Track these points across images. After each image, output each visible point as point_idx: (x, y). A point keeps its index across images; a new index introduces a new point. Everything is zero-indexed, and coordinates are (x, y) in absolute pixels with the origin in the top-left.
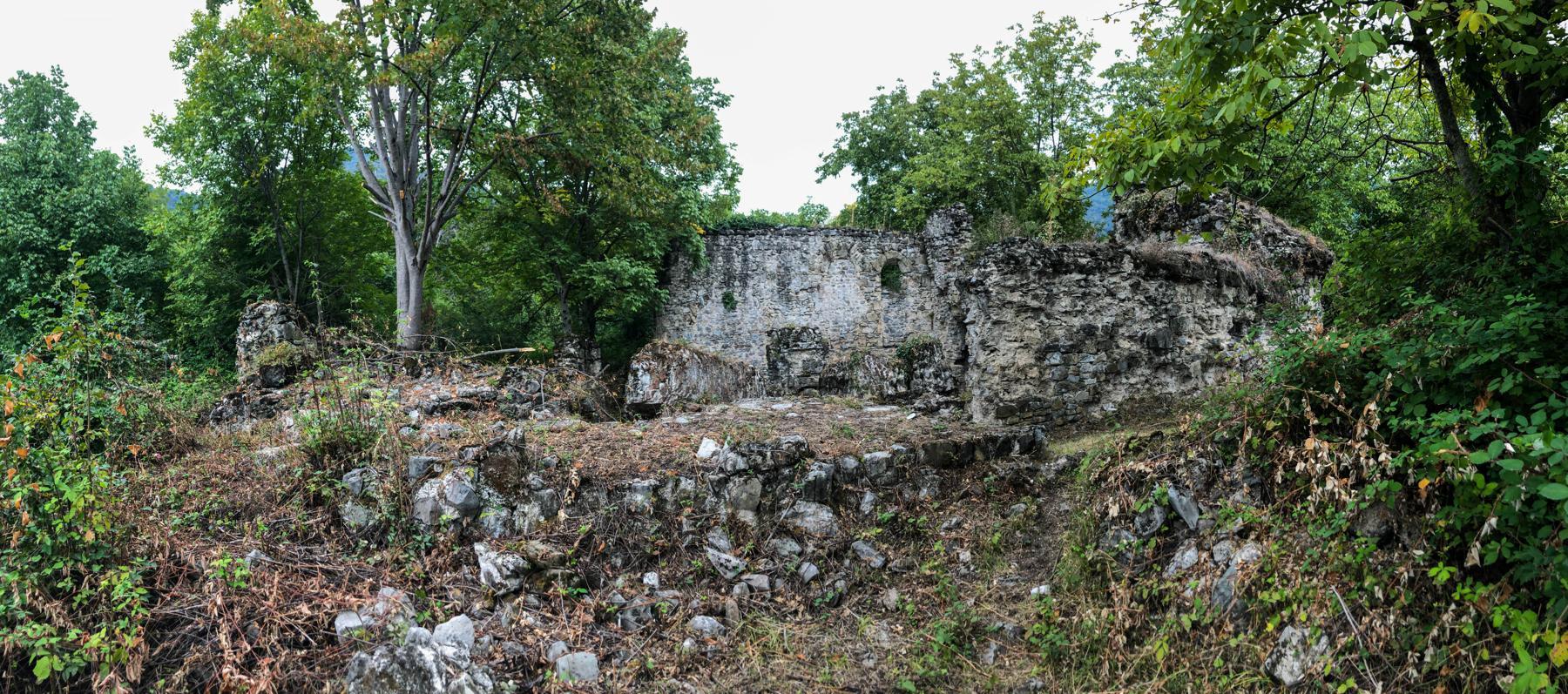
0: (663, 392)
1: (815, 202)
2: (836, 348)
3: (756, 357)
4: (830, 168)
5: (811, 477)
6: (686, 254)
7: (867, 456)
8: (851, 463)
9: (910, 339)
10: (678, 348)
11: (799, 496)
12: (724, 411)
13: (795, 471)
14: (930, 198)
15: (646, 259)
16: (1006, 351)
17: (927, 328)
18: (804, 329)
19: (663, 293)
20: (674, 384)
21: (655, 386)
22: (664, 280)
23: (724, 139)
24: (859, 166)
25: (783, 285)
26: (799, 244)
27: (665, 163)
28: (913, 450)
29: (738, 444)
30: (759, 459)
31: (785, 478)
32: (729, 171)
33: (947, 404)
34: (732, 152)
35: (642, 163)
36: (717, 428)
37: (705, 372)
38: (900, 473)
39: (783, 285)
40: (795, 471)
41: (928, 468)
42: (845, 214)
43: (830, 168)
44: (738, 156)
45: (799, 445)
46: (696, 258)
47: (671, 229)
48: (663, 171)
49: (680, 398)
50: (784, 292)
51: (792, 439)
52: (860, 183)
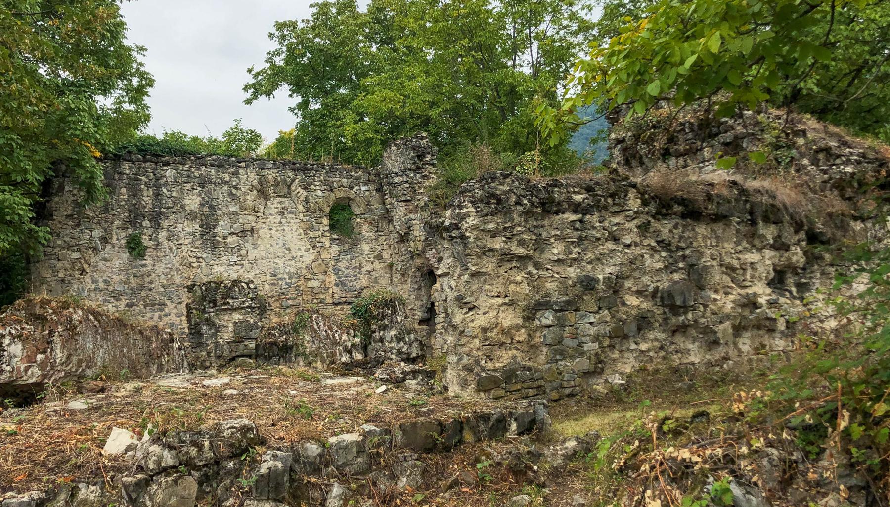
0: (42, 366)
1: (246, 126)
2: (275, 306)
3: (174, 318)
4: (262, 86)
5: (263, 470)
6: (76, 181)
7: (333, 440)
8: (313, 449)
9: (365, 294)
10: (65, 306)
11: (248, 494)
12: (138, 390)
13: (241, 463)
14: (385, 126)
15: (15, 184)
16: (485, 309)
17: (384, 281)
18: (236, 283)
19: (42, 232)
20: (59, 355)
21: (30, 359)
22: (42, 213)
23: (129, 40)
24: (298, 87)
25: (208, 226)
26: (227, 177)
27: (44, 59)
28: (388, 432)
29: (164, 433)
30: (194, 451)
31: (229, 473)
32: (135, 81)
33: (415, 374)
34: (140, 58)
35: (11, 56)
36: (135, 415)
37: (105, 338)
38: (374, 458)
39: (208, 226)
40: (241, 463)
41: (408, 453)
42: (282, 142)
43: (262, 86)
44: (150, 64)
45: (245, 430)
46: (89, 189)
47: (54, 147)
48: (42, 70)
49: (68, 374)
50: (209, 239)
51: (235, 423)
52: (299, 106)
